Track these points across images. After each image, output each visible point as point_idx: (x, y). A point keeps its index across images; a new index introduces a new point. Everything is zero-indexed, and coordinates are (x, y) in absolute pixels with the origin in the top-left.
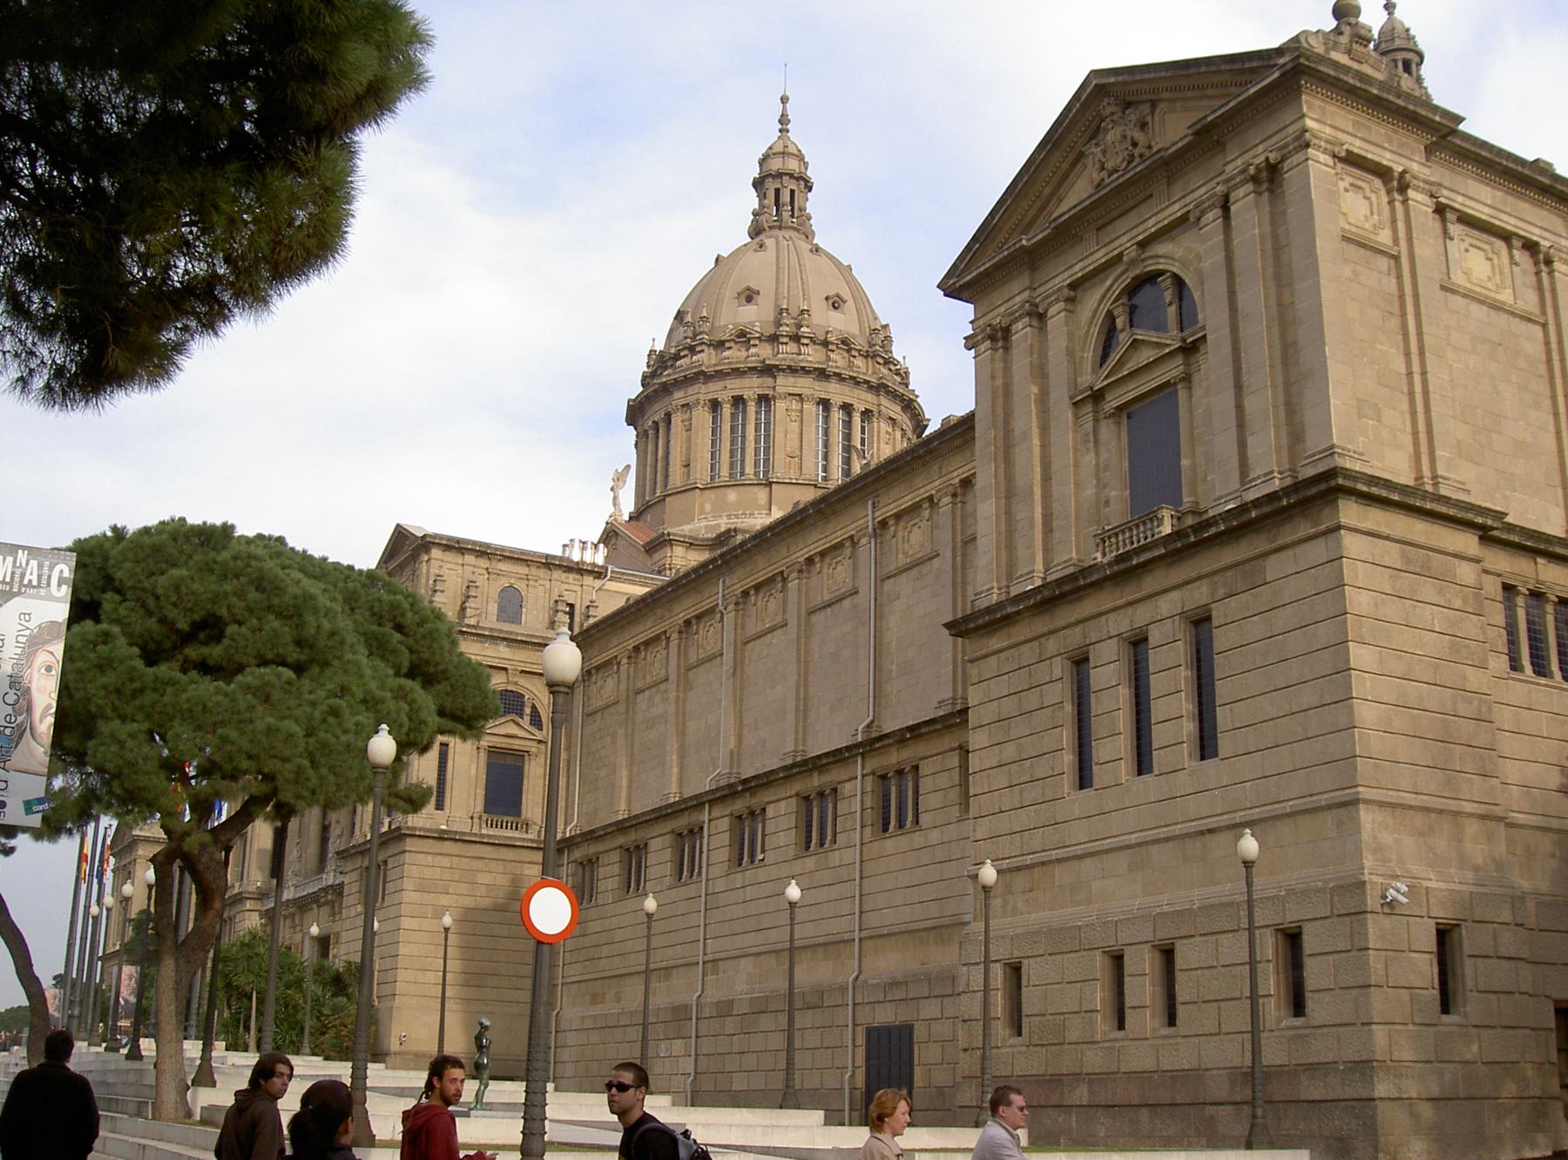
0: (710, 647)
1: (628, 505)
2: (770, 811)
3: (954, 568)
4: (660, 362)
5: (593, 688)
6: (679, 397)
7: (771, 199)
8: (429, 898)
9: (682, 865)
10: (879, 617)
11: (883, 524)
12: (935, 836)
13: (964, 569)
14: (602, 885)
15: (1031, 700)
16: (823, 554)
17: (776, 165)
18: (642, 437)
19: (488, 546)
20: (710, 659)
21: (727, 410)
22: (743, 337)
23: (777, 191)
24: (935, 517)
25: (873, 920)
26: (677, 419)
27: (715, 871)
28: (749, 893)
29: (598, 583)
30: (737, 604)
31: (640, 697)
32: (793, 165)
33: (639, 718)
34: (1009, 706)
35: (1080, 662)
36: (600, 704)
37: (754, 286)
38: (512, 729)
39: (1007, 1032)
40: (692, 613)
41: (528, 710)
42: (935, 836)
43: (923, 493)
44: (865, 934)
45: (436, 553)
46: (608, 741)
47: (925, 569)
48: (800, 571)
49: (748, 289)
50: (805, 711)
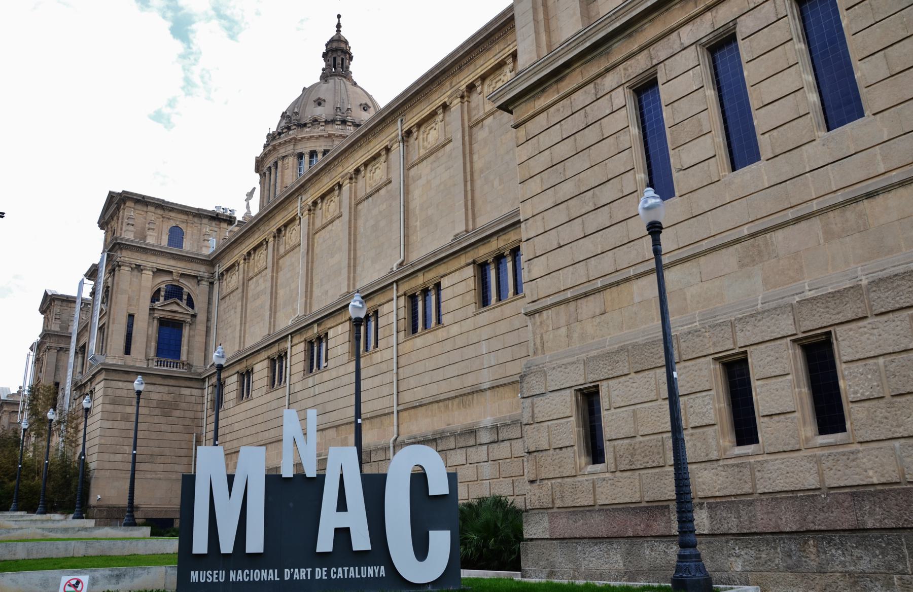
0: (292, 243)
1: (255, 210)
2: (331, 333)
3: (464, 144)
4: (271, 137)
5: (224, 283)
6: (282, 152)
7: (331, 62)
8: (119, 408)
9: (274, 378)
10: (407, 192)
11: (409, 133)
12: (455, 330)
13: (471, 144)
14: (226, 397)
15: (591, 135)
16: (366, 164)
17: (335, 45)
18: (263, 176)
19: (164, 201)
20: (293, 249)
21: (307, 158)
22: (315, 121)
23: (335, 58)
24: (447, 119)
25: (407, 397)
26: (280, 164)
27: (295, 379)
28: (317, 390)
29: (230, 228)
30: (309, 210)
31: (250, 282)
32: (343, 45)
33: (250, 295)
34: (565, 150)
35: (645, 89)
36: (229, 291)
37: (322, 97)
38: (175, 308)
39: (584, 460)
40: (282, 223)
41: (185, 297)
42: (455, 330)
43: (439, 103)
44: (401, 407)
45: (129, 204)
46: (233, 311)
47: (440, 153)
48: (351, 179)
49: (319, 99)
50: (355, 266)
